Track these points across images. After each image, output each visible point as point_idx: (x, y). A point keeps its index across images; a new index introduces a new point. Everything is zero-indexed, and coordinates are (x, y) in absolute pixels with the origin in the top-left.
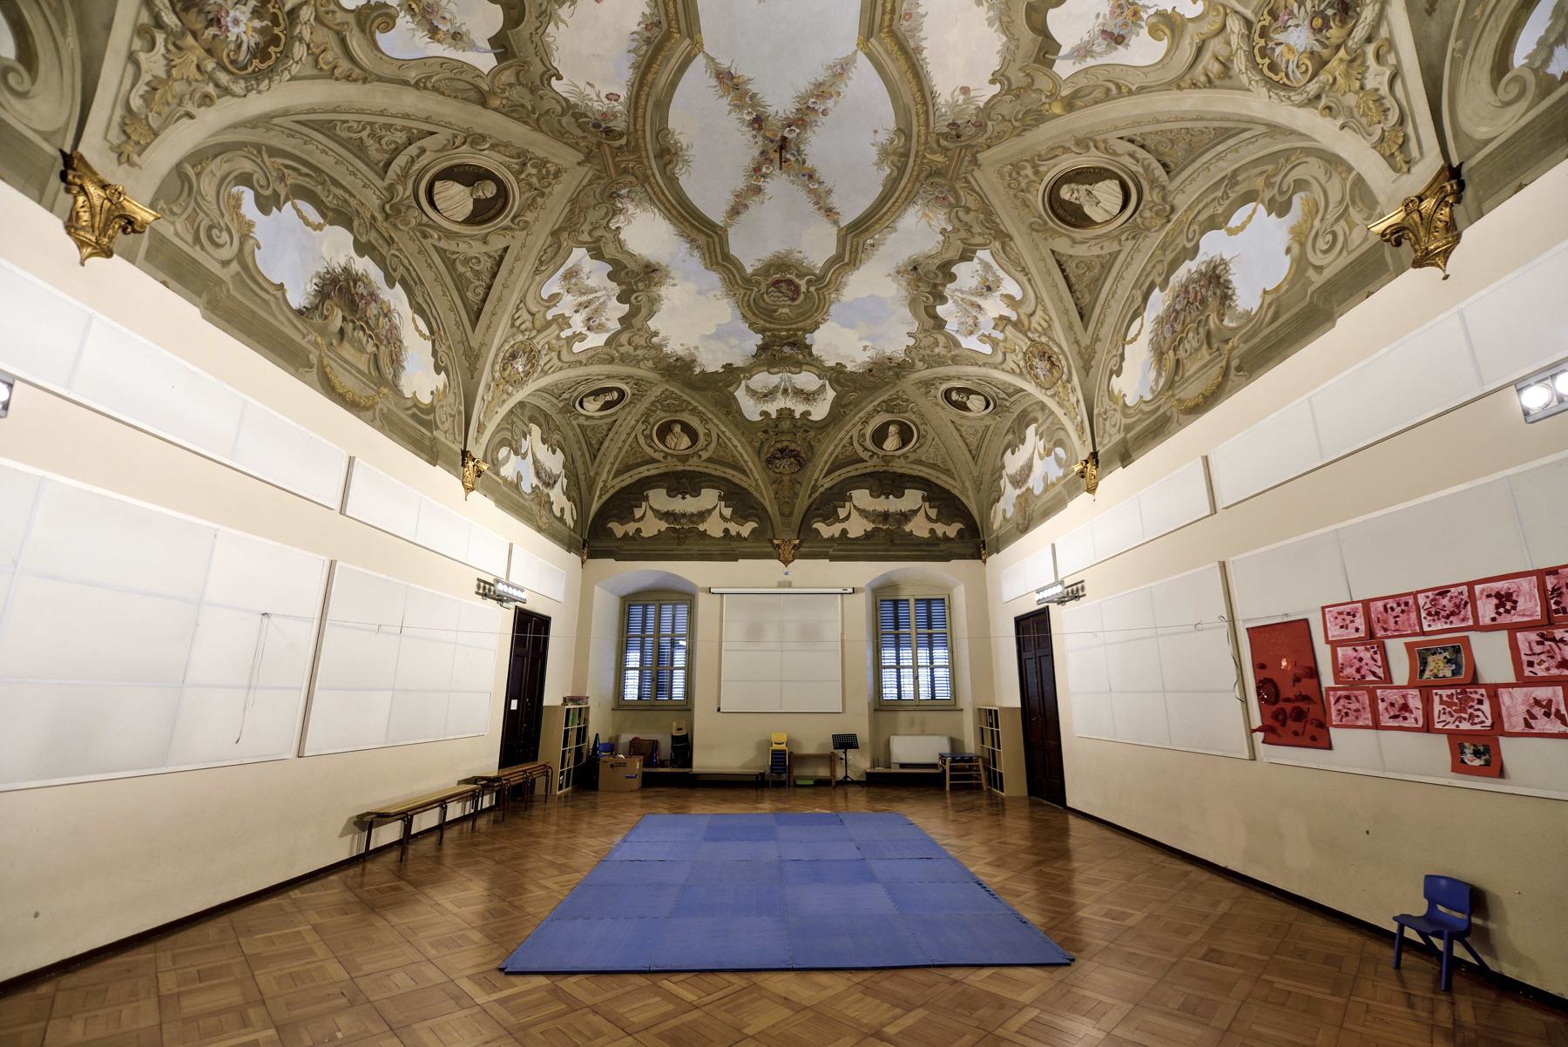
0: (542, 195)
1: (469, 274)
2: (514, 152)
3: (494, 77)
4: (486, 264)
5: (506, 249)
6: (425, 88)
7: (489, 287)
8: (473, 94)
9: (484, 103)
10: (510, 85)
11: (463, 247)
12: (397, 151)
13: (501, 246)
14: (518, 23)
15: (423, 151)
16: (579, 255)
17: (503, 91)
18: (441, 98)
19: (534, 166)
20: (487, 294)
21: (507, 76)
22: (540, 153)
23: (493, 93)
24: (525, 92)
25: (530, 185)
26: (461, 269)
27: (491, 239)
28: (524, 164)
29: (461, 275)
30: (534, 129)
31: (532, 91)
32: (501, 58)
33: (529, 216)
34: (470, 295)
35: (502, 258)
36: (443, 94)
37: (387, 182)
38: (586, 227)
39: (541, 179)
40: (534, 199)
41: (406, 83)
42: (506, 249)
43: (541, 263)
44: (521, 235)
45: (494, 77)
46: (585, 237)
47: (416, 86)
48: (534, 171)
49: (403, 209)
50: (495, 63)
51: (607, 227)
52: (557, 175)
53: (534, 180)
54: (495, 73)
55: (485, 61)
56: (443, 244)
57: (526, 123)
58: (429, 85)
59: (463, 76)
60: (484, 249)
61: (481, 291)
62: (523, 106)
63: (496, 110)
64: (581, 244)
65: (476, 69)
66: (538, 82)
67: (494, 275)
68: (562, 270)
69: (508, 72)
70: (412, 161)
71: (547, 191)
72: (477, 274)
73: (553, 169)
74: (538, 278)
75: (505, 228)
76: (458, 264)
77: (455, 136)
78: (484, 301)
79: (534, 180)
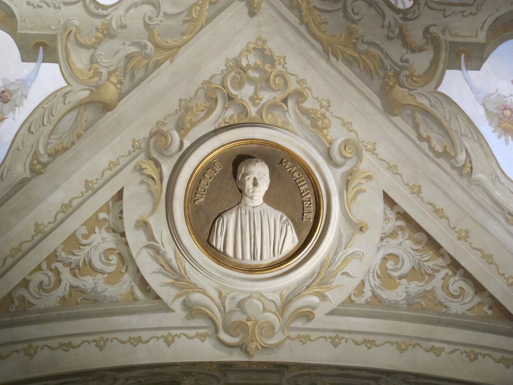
0: (300, 95)
1: (415, 287)
2: (201, 102)
3: (73, 75)
4: (405, 246)
5: (388, 200)
6: (44, 165)
7: (455, 265)
8: (88, 114)
9: (107, 107)
10: (93, 61)
11: (357, 270)
12: (126, 259)
13: (380, 205)
14: (11, 15)
15: (144, 225)
16: (456, 85)
17: (97, 73)
18: (68, 154)
19: (239, 85)
20: (468, 276)
21: (80, 59)
22: (215, 66)
23: (95, 89)
24: (108, 46)
25: (272, 106)
26: (397, 295)
27: (358, 214)
28: (230, 98)
29: (411, 302)
30: (172, 57)
31: (108, 33)
32: (51, 56)
33: (337, 135)
34: (456, 307)
35: (404, 216)
36: (65, 149)
37: (177, 306)
38: (396, 51)
39: (266, 82)
40: (305, 112)
41: (23, 183)
42: (388, 200)
43: (445, 155)
44: (367, 163)
45: (73, 75)
46: (421, 62)
47: (35, 172)
48: (248, 90)
49: (238, 317)
50: (56, 66)
51: (405, 14)
52: (269, 59)
53: (266, 96)
54: (69, 72)
55: (48, 78)
56: (336, 297)
57: (158, 65)
58: (45, 159)
59: (58, 114)
60: (373, 235)
61: (457, 284)
62: (129, 58)
63: (121, 97)
64: (433, 74)
65: (54, 94)
66: (98, 22)
67: (433, 245)
68: (486, 129)
69: (74, 58)
70: (157, 252)
71: (293, 86)
72: (416, 273)
73: (253, 59)
74: (479, 176)
75: (346, 182)
76: (385, 294)
77: (140, 169)
78: (479, 288)
79: (266, 96)
